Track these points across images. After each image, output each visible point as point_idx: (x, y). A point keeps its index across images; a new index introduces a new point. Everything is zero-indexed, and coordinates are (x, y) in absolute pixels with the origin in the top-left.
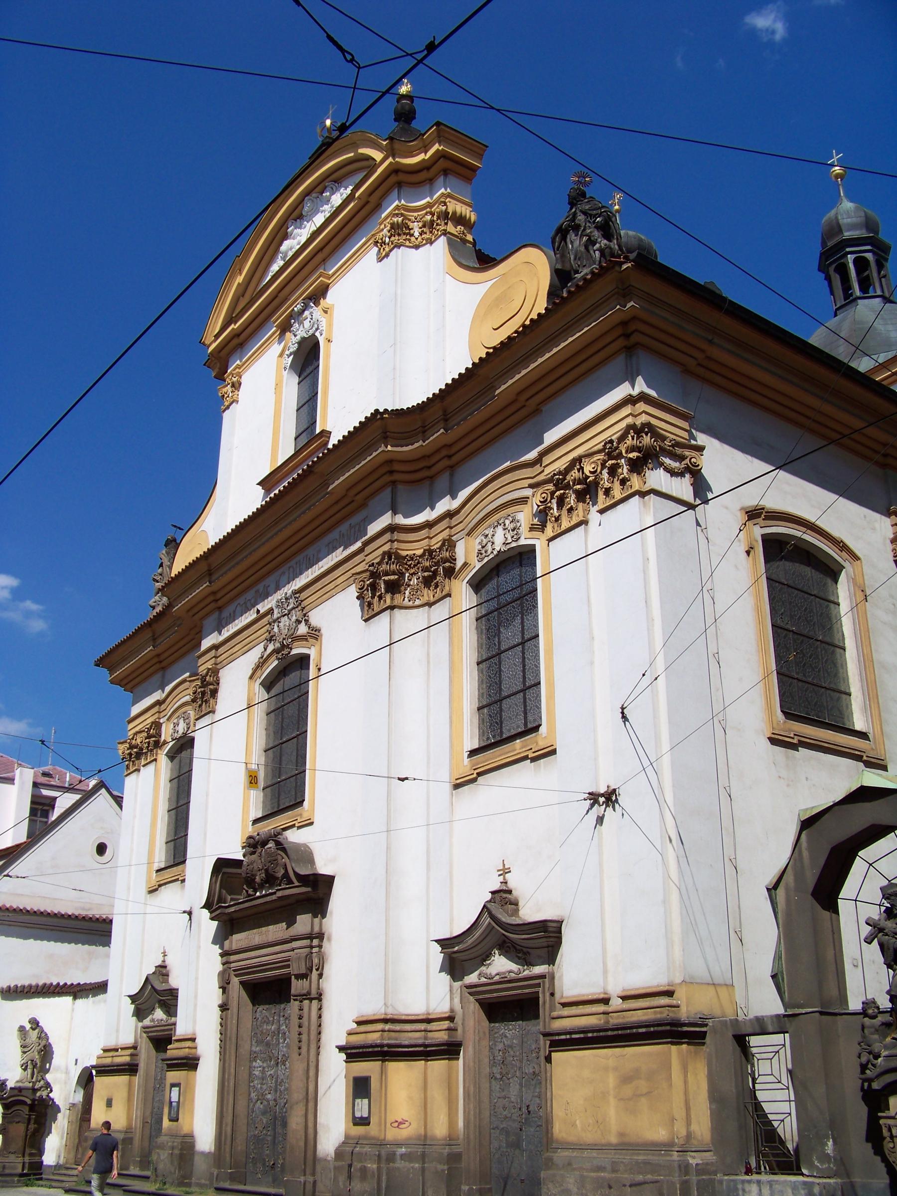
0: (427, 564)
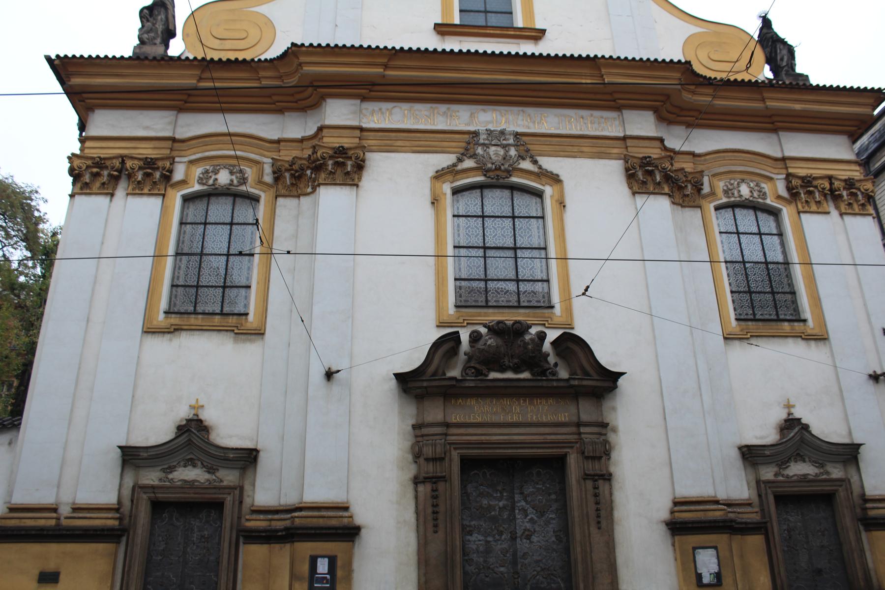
0: (684, 179)
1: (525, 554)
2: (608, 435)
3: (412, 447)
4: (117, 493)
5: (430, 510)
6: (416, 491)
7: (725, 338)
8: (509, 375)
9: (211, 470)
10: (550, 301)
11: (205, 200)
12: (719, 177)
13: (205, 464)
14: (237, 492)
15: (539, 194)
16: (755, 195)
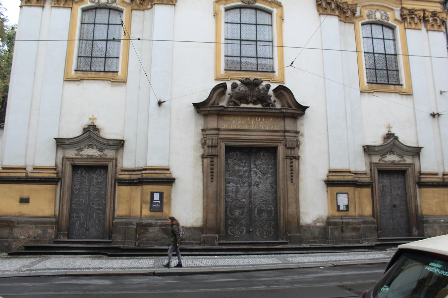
0: (347, 8)
1: (255, 193)
2: (299, 137)
3: (201, 140)
4: (54, 161)
5: (209, 171)
6: (203, 162)
7: (361, 92)
8: (251, 106)
9: (101, 150)
10: (273, 69)
11: (94, 11)
12: (365, 7)
13: (98, 147)
14: (114, 161)
15: (270, 13)
16: (384, 18)
